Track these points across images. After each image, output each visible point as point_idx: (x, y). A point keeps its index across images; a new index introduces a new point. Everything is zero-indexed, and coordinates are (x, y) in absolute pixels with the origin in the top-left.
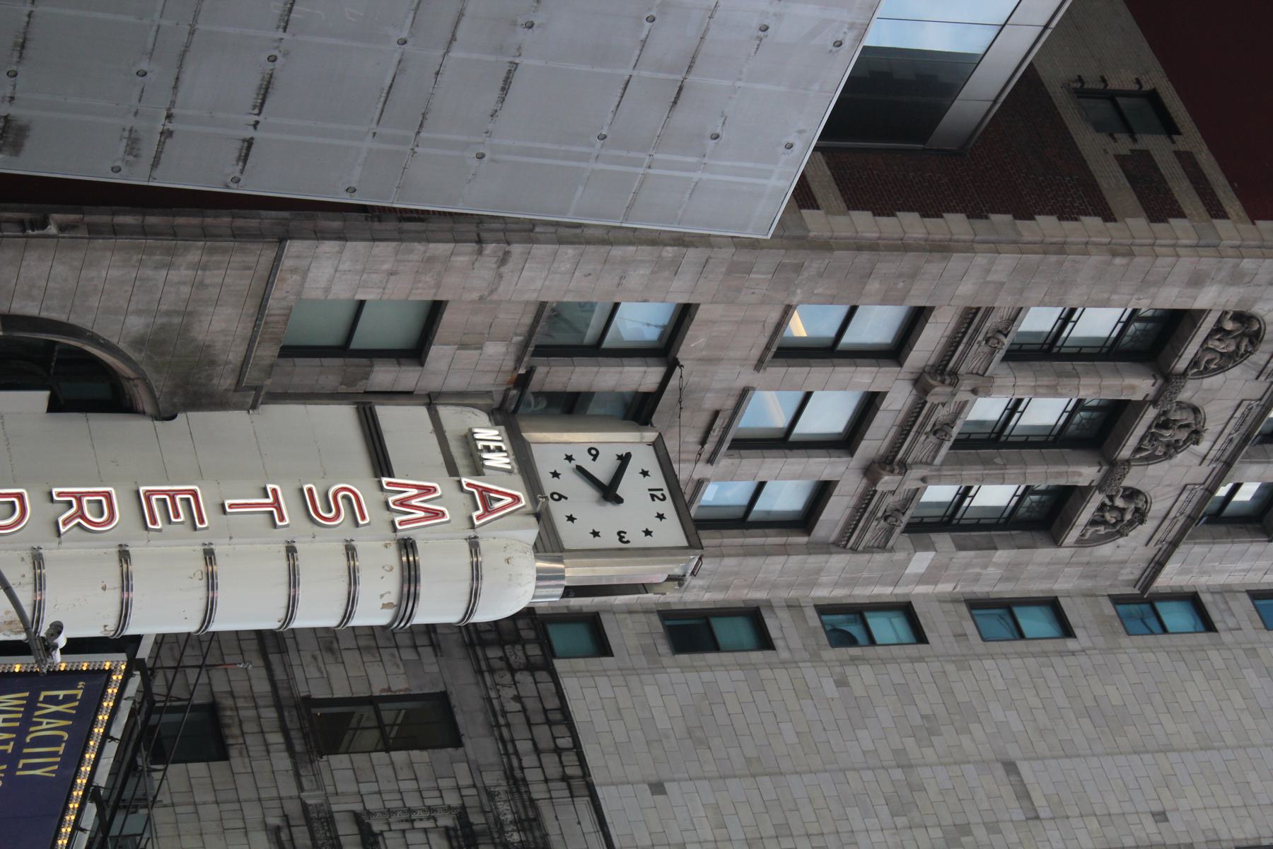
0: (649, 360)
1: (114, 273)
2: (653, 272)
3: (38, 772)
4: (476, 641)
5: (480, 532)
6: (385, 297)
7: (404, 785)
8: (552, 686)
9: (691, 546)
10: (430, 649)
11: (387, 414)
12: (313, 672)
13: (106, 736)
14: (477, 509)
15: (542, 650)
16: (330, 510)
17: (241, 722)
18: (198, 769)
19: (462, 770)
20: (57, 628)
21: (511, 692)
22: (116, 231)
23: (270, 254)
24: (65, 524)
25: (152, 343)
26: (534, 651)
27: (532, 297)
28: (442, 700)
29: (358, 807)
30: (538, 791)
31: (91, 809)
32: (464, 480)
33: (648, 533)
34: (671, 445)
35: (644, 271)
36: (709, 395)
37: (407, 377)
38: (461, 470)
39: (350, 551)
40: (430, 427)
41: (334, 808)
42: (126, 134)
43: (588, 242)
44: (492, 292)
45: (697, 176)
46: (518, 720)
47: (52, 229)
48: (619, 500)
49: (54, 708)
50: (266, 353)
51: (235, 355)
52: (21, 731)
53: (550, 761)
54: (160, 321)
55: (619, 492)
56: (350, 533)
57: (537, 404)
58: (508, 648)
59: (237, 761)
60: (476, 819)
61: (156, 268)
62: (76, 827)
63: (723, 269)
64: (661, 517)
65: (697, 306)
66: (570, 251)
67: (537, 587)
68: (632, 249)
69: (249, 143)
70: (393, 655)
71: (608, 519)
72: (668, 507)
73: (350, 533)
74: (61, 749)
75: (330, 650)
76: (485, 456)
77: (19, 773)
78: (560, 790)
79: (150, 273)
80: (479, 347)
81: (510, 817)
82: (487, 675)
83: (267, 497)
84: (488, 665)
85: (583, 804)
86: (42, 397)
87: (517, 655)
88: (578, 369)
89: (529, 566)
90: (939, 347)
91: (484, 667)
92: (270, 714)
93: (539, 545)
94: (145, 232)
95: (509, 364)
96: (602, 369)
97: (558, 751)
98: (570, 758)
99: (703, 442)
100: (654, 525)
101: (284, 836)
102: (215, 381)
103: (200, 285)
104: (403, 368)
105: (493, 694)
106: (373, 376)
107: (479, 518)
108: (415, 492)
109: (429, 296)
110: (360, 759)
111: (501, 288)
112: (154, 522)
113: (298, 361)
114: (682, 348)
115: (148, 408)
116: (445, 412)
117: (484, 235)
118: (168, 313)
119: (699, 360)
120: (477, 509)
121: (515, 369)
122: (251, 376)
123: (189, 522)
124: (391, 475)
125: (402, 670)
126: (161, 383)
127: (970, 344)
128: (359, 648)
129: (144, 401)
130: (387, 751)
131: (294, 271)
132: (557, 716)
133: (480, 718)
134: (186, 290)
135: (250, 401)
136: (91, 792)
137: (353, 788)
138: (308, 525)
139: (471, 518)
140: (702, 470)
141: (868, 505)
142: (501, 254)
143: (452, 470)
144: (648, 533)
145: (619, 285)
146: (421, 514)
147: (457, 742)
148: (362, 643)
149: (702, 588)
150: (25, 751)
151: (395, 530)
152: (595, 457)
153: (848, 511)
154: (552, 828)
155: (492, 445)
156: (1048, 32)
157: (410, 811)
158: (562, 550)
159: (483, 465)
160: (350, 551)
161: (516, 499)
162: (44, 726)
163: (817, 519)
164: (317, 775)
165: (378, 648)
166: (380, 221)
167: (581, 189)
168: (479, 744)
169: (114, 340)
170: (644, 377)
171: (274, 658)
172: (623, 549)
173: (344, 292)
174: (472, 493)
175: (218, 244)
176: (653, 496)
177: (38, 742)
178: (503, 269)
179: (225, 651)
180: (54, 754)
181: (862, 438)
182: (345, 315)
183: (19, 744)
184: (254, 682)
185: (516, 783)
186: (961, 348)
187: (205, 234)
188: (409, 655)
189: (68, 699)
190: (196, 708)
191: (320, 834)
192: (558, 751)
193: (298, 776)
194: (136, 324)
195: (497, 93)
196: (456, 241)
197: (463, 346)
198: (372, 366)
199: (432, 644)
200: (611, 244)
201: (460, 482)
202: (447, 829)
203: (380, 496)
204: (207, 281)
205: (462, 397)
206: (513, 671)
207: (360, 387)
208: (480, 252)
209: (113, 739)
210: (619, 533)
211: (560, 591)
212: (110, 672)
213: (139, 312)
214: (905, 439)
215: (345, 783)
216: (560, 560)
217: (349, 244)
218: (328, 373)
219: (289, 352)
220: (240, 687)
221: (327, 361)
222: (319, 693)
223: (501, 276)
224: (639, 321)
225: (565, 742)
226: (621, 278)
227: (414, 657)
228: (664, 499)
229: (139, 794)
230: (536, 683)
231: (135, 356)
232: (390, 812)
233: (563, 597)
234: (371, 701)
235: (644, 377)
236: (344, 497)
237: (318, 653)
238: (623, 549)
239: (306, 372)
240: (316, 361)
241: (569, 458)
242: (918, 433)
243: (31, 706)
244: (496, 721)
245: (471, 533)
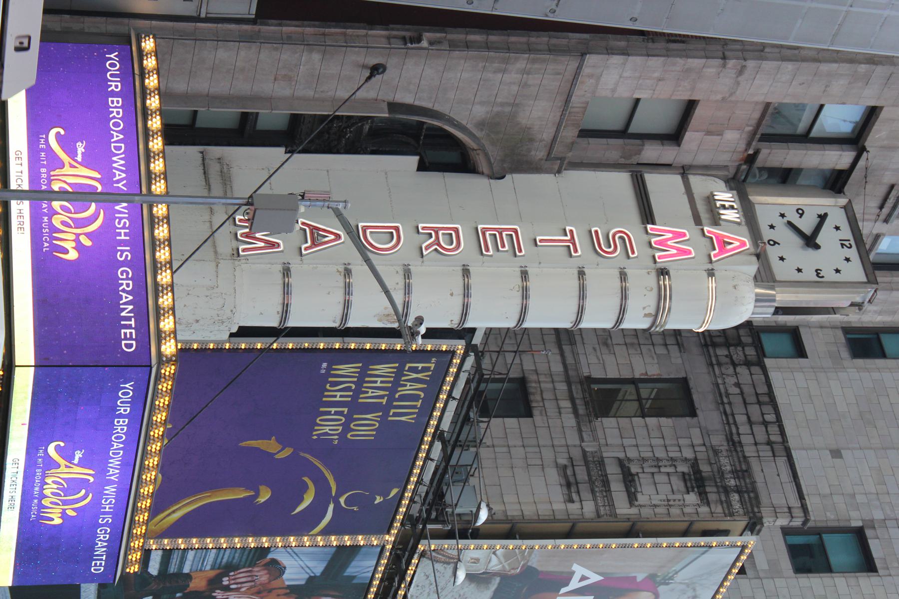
0: (844, 146)
1: (465, 75)
2: (850, 83)
3: (403, 419)
4: (709, 343)
5: (715, 266)
6: (655, 96)
7: (655, 442)
8: (762, 377)
9: (869, 282)
10: (676, 347)
11: (652, 180)
12: (593, 359)
13: (450, 396)
14: (714, 249)
15: (757, 351)
16: (610, 247)
17: (542, 392)
18: (511, 422)
19: (696, 433)
20: (420, 320)
21: (733, 380)
22: (468, 46)
23: (573, 64)
24: (426, 249)
25: (489, 125)
26: (751, 352)
27: (761, 98)
28: (684, 384)
29: (621, 455)
30: (749, 451)
31: (438, 446)
32: (706, 229)
33: (837, 271)
34: (858, 208)
35: (843, 82)
36: (887, 173)
37: (667, 153)
38: (704, 221)
39: (623, 276)
40: (683, 189)
41: (605, 455)
43: (804, 60)
44: (731, 95)
45: (886, 13)
46: (737, 400)
47: (424, 44)
48: (817, 247)
49: (415, 376)
50: (569, 133)
51: (547, 135)
52: (392, 390)
53: (759, 430)
54: (496, 109)
55: (818, 241)
56: (624, 263)
57: (761, 176)
58: (732, 348)
59: (538, 418)
60: (705, 468)
61: (495, 72)
62: (428, 458)
64: (847, 260)
65: (881, 108)
66: (789, 66)
67: (755, 307)
68: (835, 65)
70: (650, 350)
71: (809, 260)
72: (853, 253)
73: (624, 263)
74: (419, 404)
75: (606, 344)
76: (722, 212)
77: (390, 419)
78: (766, 451)
79: (490, 75)
80: (720, 134)
81: (729, 468)
82: (716, 367)
83: (566, 235)
84: (717, 360)
85: (782, 462)
86: (414, 160)
87: (738, 354)
88: (792, 152)
89: (749, 292)
91: (714, 362)
92: (562, 387)
93: (758, 277)
94: (488, 47)
95: (742, 146)
96: (809, 152)
97: (765, 424)
98: (774, 429)
99: (881, 207)
100: (843, 265)
101: (569, 472)
102: (533, 153)
103: (524, 85)
104: (666, 147)
105: (720, 381)
106: (643, 152)
107: (715, 256)
108: (670, 235)
109: (687, 98)
110: (624, 422)
111: (738, 92)
112: (487, 250)
113: (591, 140)
114: (869, 138)
115: (486, 170)
116: (694, 180)
117: (727, 53)
118: (502, 105)
119: (882, 147)
120: (714, 249)
121: (746, 150)
122: (558, 150)
123: (511, 252)
124: (653, 223)
125: (656, 361)
126: (495, 153)
128: (626, 344)
129: (483, 166)
130: (643, 417)
131: (591, 76)
132: (766, 399)
133: (710, 397)
134: (515, 88)
135: (556, 167)
136: (438, 435)
137: (618, 441)
138: (593, 256)
139: (709, 256)
140: (880, 227)
142: (739, 67)
143: (698, 221)
144: (837, 271)
145: (824, 91)
146: (675, 251)
147: (693, 413)
148: (628, 341)
149: (875, 312)
150: (395, 403)
151: (655, 262)
152: (801, 215)
154: (759, 478)
155: (727, 204)
157: (658, 459)
158: (775, 281)
159: (720, 218)
160: (623, 276)
161: (743, 244)
162: (408, 387)
164: (593, 431)
165: (639, 344)
166: (653, 42)
167: (800, 21)
168: (709, 414)
169: (464, 122)
170: (840, 158)
171: (567, 348)
172: (819, 281)
173: (626, 92)
174: (711, 238)
175: (538, 56)
176: (842, 245)
177: (403, 398)
178: (740, 79)
179: (532, 342)
180: (414, 407)
182: (626, 108)
183: (391, 398)
184: (552, 364)
185: (734, 444)
187: (530, 49)
188: (661, 350)
189: (424, 370)
190: (511, 380)
191: (594, 473)
192: (765, 424)
193: (580, 431)
194: (480, 111)
196: (707, 58)
197: (709, 133)
198: (643, 145)
199: (678, 344)
200: (820, 61)
201: (702, 230)
202: (684, 473)
203: (646, 237)
204: (530, 82)
205: (706, 169)
206: (734, 365)
207: (634, 160)
208: (724, 66)
209: (454, 399)
210: (817, 270)
211: (772, 310)
212: (452, 353)
213: (482, 103)
215: (613, 437)
216: (772, 288)
217: (630, 58)
218: (612, 149)
219: (586, 133)
220: (542, 367)
221: (612, 141)
222: (597, 374)
223: (738, 83)
224: (838, 118)
225: (771, 417)
226: (826, 86)
227: (665, 352)
228: (851, 247)
229: (471, 437)
230: (751, 374)
231: (478, 134)
232: (644, 460)
233: (774, 314)
234: (633, 381)
235: (840, 158)
236: (621, 237)
237: (597, 346)
238: (819, 281)
239: (597, 148)
240: (604, 141)
241: (782, 215)
243: (399, 373)
244: (721, 399)
245: (710, 266)
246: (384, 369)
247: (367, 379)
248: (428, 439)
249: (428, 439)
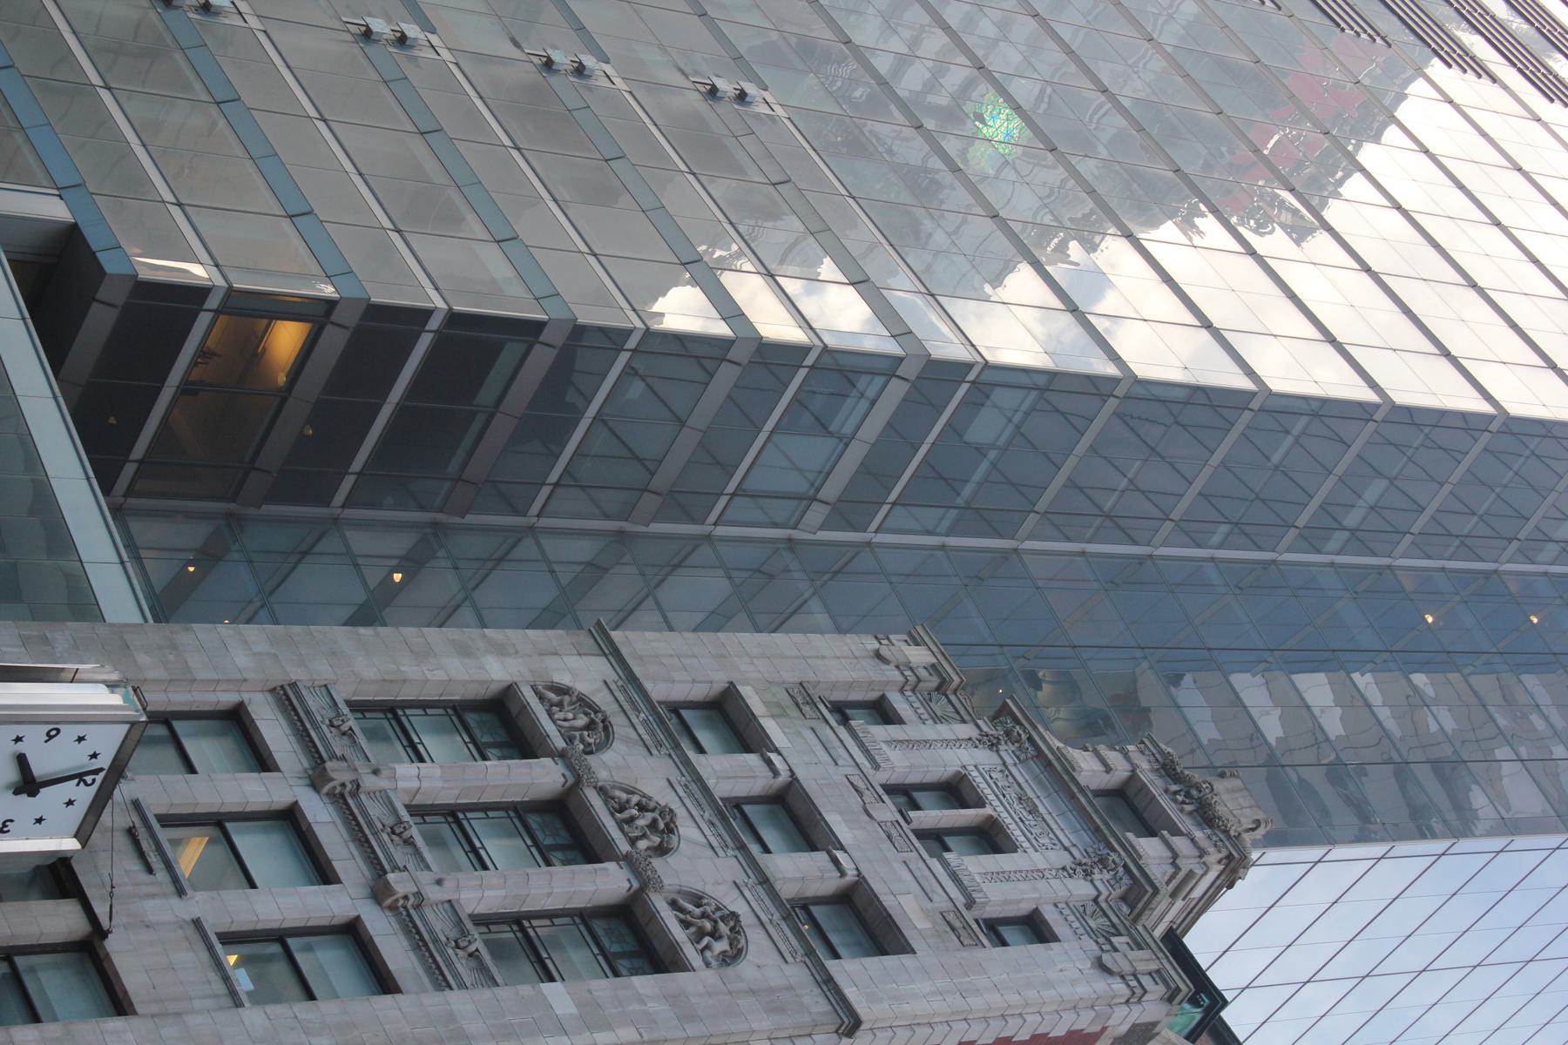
90: (296, 746)
127: (317, 728)
141: (418, 932)
153: (411, 954)
156: (128, 565)
163: (389, 972)
181: (329, 862)
186: (313, 734)
214: (371, 847)
242: (375, 834)
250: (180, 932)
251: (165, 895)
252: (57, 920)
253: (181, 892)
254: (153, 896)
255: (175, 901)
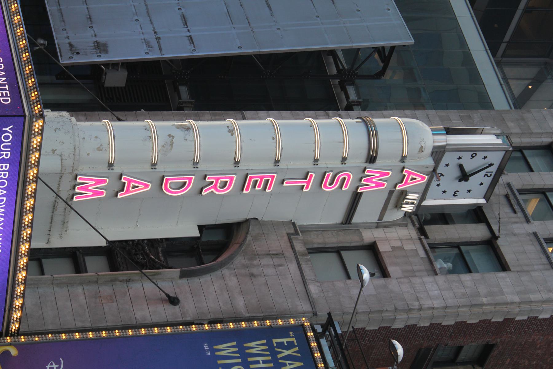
42: (143, 41)
49: (286, 353)
63: (438, 119)
69: (190, 37)
156: (504, 86)
195: (267, 9)
246: (256, 346)
247: (250, 359)
248: (314, 344)
249: (314, 344)
250: (528, 238)
251: (521, 222)
252: (478, 232)
253: (528, 221)
254: (516, 223)
255: (526, 225)
